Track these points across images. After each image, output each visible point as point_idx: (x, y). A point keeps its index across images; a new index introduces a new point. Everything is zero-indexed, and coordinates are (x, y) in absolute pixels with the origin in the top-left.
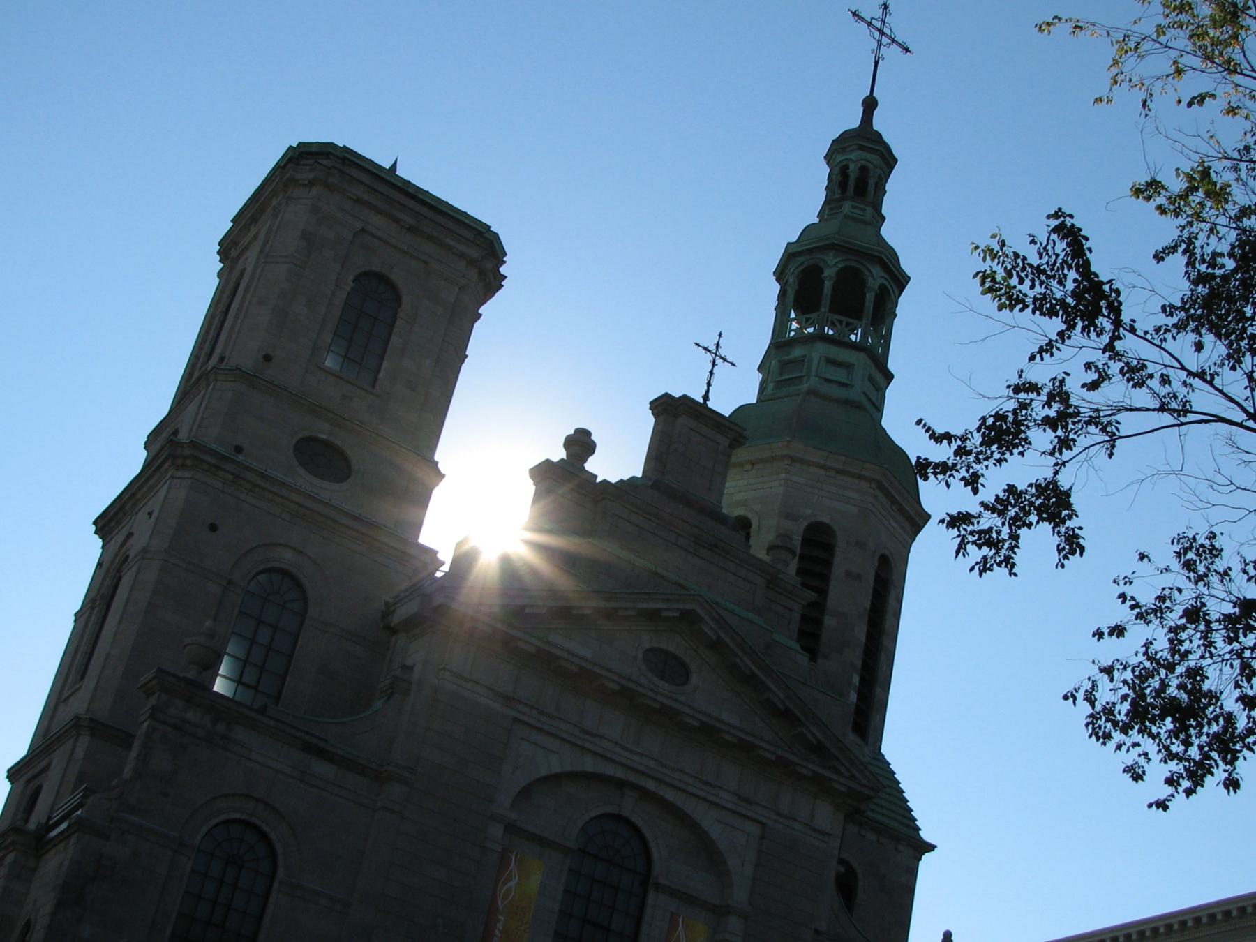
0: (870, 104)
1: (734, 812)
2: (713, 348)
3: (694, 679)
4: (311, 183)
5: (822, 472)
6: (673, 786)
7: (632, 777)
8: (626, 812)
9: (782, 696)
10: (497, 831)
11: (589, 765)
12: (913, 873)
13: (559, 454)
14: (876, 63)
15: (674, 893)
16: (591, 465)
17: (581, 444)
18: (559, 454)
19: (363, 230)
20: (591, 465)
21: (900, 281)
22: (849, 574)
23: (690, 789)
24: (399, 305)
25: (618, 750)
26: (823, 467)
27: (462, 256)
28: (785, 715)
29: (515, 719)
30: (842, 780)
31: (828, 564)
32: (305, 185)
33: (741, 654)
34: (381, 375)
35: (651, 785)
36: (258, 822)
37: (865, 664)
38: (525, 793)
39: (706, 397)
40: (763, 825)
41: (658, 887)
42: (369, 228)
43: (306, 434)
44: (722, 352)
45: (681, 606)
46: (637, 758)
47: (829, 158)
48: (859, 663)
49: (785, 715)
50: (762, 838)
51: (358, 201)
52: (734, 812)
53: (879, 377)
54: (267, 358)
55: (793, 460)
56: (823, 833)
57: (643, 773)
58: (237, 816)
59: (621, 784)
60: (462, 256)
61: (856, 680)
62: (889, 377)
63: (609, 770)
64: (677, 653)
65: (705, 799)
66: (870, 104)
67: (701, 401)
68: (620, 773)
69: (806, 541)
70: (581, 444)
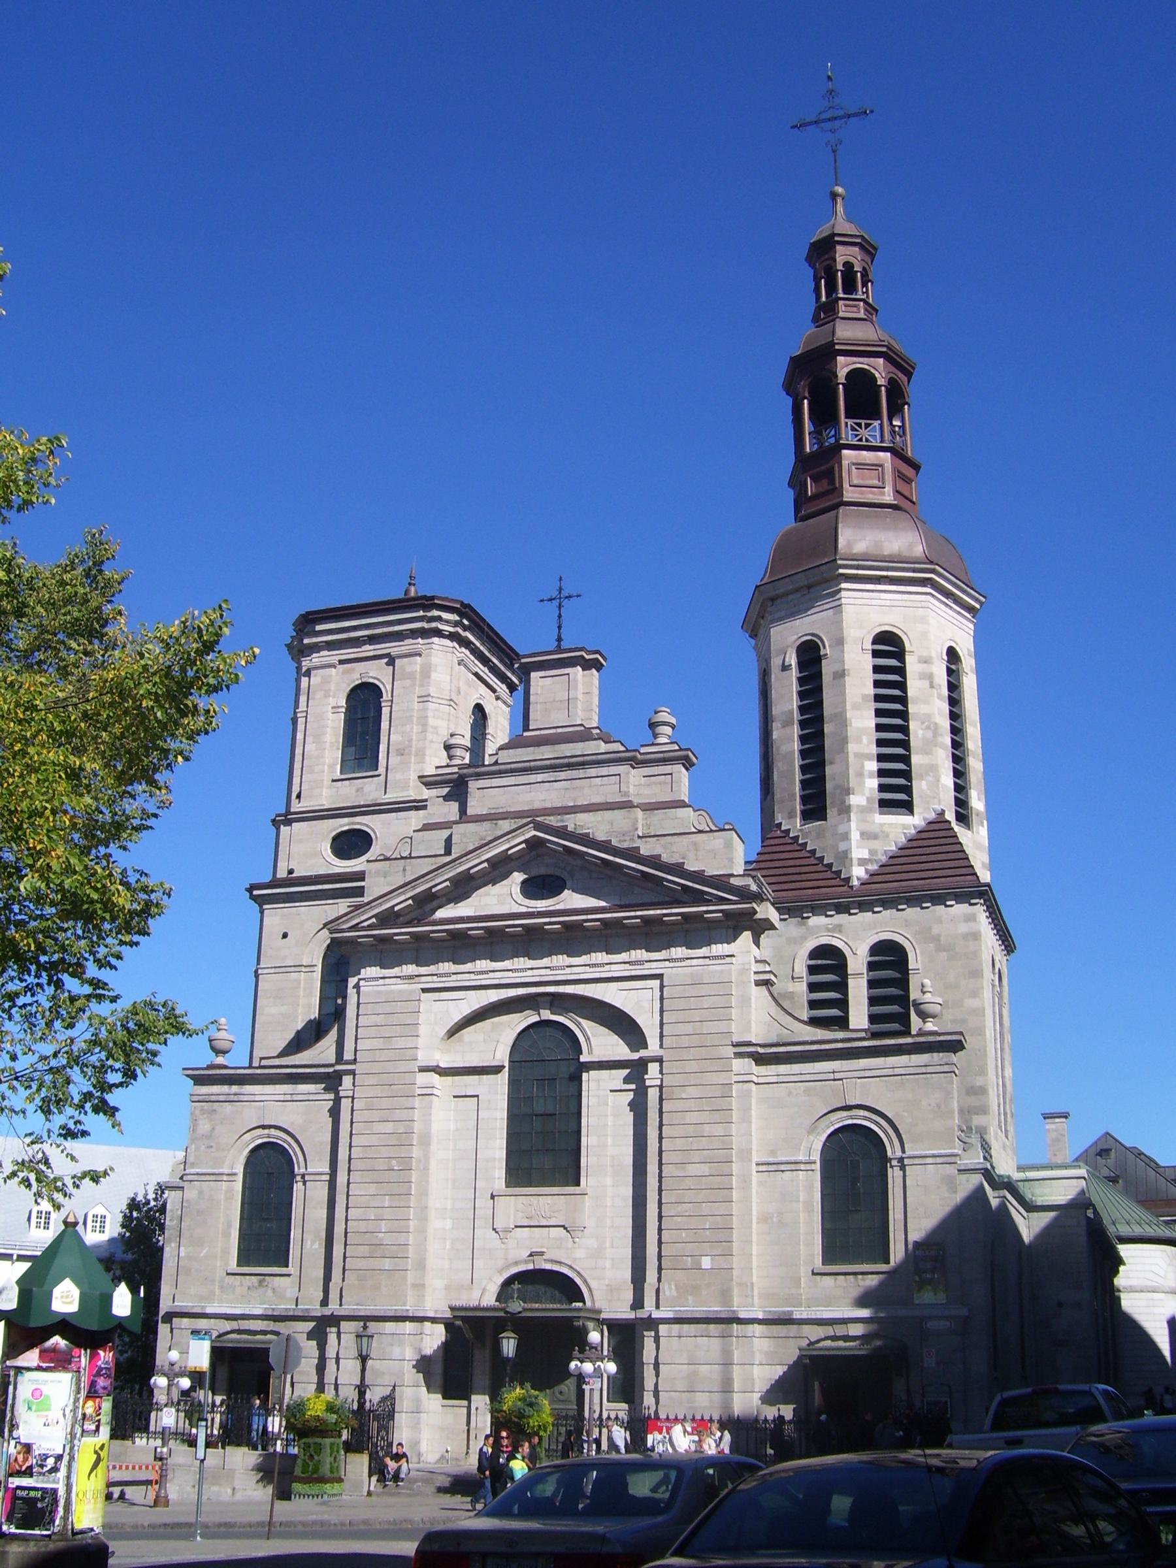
5: (798, 595)
11: (494, 996)
14: (834, 151)
25: (510, 974)
26: (796, 591)
29: (424, 990)
36: (275, 1140)
44: (555, 594)
45: (522, 839)
46: (529, 973)
48: (874, 750)
50: (662, 987)
51: (330, 646)
55: (773, 600)
58: (260, 1141)
61: (873, 766)
64: (550, 871)
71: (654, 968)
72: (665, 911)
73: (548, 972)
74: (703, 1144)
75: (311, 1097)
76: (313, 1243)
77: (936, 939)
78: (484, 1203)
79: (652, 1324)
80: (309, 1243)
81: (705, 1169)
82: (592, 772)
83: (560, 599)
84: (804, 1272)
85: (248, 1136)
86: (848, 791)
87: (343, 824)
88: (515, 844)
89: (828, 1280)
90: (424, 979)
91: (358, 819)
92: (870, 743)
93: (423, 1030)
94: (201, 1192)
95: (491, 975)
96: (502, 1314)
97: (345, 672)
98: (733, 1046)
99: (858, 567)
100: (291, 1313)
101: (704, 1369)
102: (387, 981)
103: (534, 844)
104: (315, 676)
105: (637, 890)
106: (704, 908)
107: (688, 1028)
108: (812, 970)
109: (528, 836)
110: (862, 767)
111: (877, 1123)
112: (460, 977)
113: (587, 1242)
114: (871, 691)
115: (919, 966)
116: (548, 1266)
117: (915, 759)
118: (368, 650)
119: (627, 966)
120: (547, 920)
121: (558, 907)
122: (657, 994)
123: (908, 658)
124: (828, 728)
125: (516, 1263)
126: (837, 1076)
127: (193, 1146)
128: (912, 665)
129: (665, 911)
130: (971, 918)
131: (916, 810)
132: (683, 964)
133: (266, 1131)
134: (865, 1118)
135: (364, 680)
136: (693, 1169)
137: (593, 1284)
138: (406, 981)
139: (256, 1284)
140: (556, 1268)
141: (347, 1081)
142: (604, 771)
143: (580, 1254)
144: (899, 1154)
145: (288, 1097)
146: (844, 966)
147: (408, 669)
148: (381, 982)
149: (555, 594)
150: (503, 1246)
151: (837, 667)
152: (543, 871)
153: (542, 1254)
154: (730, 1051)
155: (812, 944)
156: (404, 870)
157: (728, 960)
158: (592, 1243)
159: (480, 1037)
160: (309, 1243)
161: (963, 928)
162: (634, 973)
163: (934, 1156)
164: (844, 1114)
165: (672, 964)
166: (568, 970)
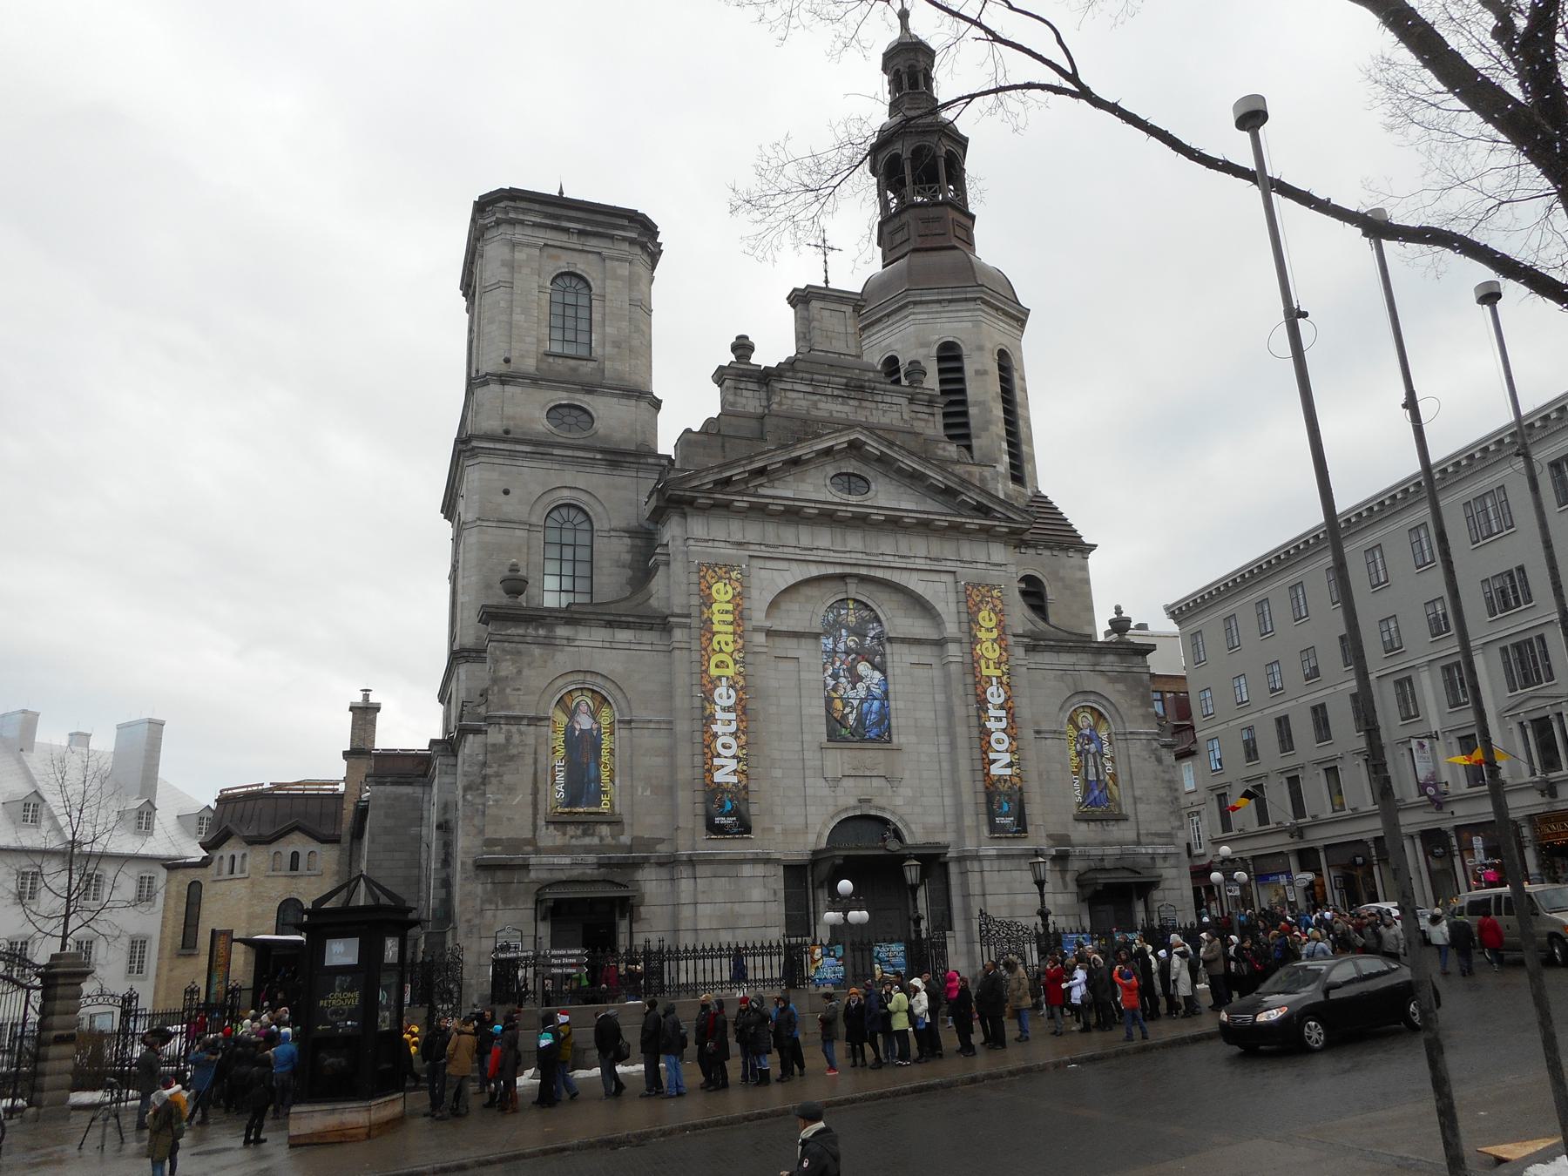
2: (820, 243)
3: (873, 486)
4: (498, 223)
5: (938, 305)
6: (879, 567)
7: (848, 570)
9: (941, 479)
10: (760, 638)
11: (814, 571)
12: (1085, 568)
13: (728, 358)
15: (903, 641)
16: (755, 359)
17: (743, 347)
18: (728, 358)
19: (545, 245)
20: (755, 359)
21: (962, 142)
22: (978, 373)
23: (893, 565)
24: (591, 290)
25: (832, 554)
26: (939, 302)
27: (624, 239)
28: (949, 493)
29: (750, 556)
30: (1002, 524)
31: (960, 370)
32: (493, 227)
33: (901, 458)
34: (593, 345)
35: (863, 571)
37: (1009, 433)
38: (774, 604)
39: (826, 282)
40: (954, 572)
41: (890, 640)
42: (550, 242)
43: (552, 404)
44: (828, 244)
45: (846, 439)
46: (848, 555)
47: (885, 69)
48: (1004, 433)
49: (949, 493)
51: (535, 225)
53: (963, 220)
54: (507, 361)
55: (915, 303)
56: (1001, 565)
58: (574, 687)
59: (842, 577)
60: (624, 239)
61: (1005, 446)
62: (972, 218)
63: (831, 570)
65: (906, 569)
67: (824, 285)
68: (839, 570)
69: (940, 359)
70: (743, 347)
71: (949, 566)
72: (968, 521)
73: (865, 557)
75: (632, 647)
76: (644, 790)
77: (1062, 579)
78: (812, 757)
79: (978, 858)
80: (640, 790)
82: (879, 398)
84: (1071, 817)
85: (560, 682)
86: (996, 461)
87: (562, 397)
88: (840, 441)
89: (1083, 826)
90: (752, 547)
91: (578, 396)
93: (755, 593)
94: (508, 738)
95: (815, 552)
96: (882, 852)
97: (551, 257)
98: (1014, 635)
99: (992, 296)
100: (630, 861)
101: (1020, 898)
102: (716, 544)
103: (855, 446)
104: (520, 251)
105: (929, 501)
106: (997, 523)
109: (852, 437)
111: (1104, 706)
112: (785, 550)
113: (905, 791)
115: (1054, 598)
116: (873, 812)
117: (1024, 448)
118: (574, 242)
119: (929, 562)
120: (875, 511)
121: (866, 503)
122: (951, 586)
124: (972, 411)
125: (846, 810)
126: (1077, 668)
127: (496, 688)
129: (968, 521)
131: (1028, 485)
132: (971, 566)
133: (580, 677)
134: (1095, 702)
135: (571, 270)
137: (913, 827)
138: (735, 547)
139: (579, 832)
140: (879, 814)
141: (678, 634)
142: (888, 399)
143: (899, 801)
144: (1122, 731)
145: (608, 645)
147: (619, 272)
148: (710, 544)
149: (828, 244)
150: (833, 794)
151: (979, 367)
152: (850, 471)
153: (869, 801)
156: (723, 446)
157: (1003, 568)
158: (909, 792)
159: (796, 607)
160: (640, 790)
162: (933, 568)
163: (1146, 733)
164: (1081, 697)
165: (962, 565)
166: (880, 558)
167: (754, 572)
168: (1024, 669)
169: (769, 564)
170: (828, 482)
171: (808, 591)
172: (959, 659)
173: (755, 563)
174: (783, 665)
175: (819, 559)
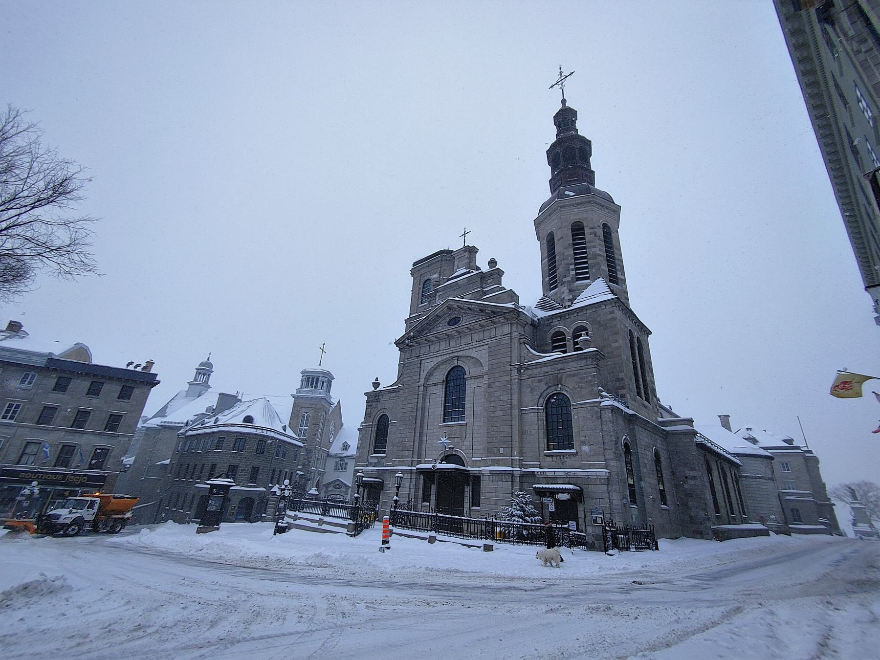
0: (564, 101)
1: (479, 346)
8: (456, 365)
11: (440, 359)
14: (563, 90)
25: (445, 351)
29: (421, 360)
35: (456, 354)
38: (430, 374)
46: (449, 350)
52: (479, 346)
57: (453, 353)
66: (564, 101)
74: (501, 403)
81: (501, 413)
83: (465, 235)
89: (549, 459)
90: (421, 357)
92: (571, 259)
93: (422, 372)
107: (496, 361)
108: (554, 342)
110: (569, 267)
114: (571, 241)
116: (454, 453)
123: (585, 228)
128: (587, 231)
130: (613, 312)
132: (495, 339)
136: (497, 414)
143: (464, 448)
146: (564, 339)
154: (509, 368)
155: (552, 331)
157: (509, 335)
161: (610, 317)
162: (480, 345)
167: (422, 365)
168: (517, 380)
169: (427, 361)
170: (447, 324)
171: (441, 367)
172: (487, 382)
173: (423, 362)
174: (433, 396)
175: (440, 354)
